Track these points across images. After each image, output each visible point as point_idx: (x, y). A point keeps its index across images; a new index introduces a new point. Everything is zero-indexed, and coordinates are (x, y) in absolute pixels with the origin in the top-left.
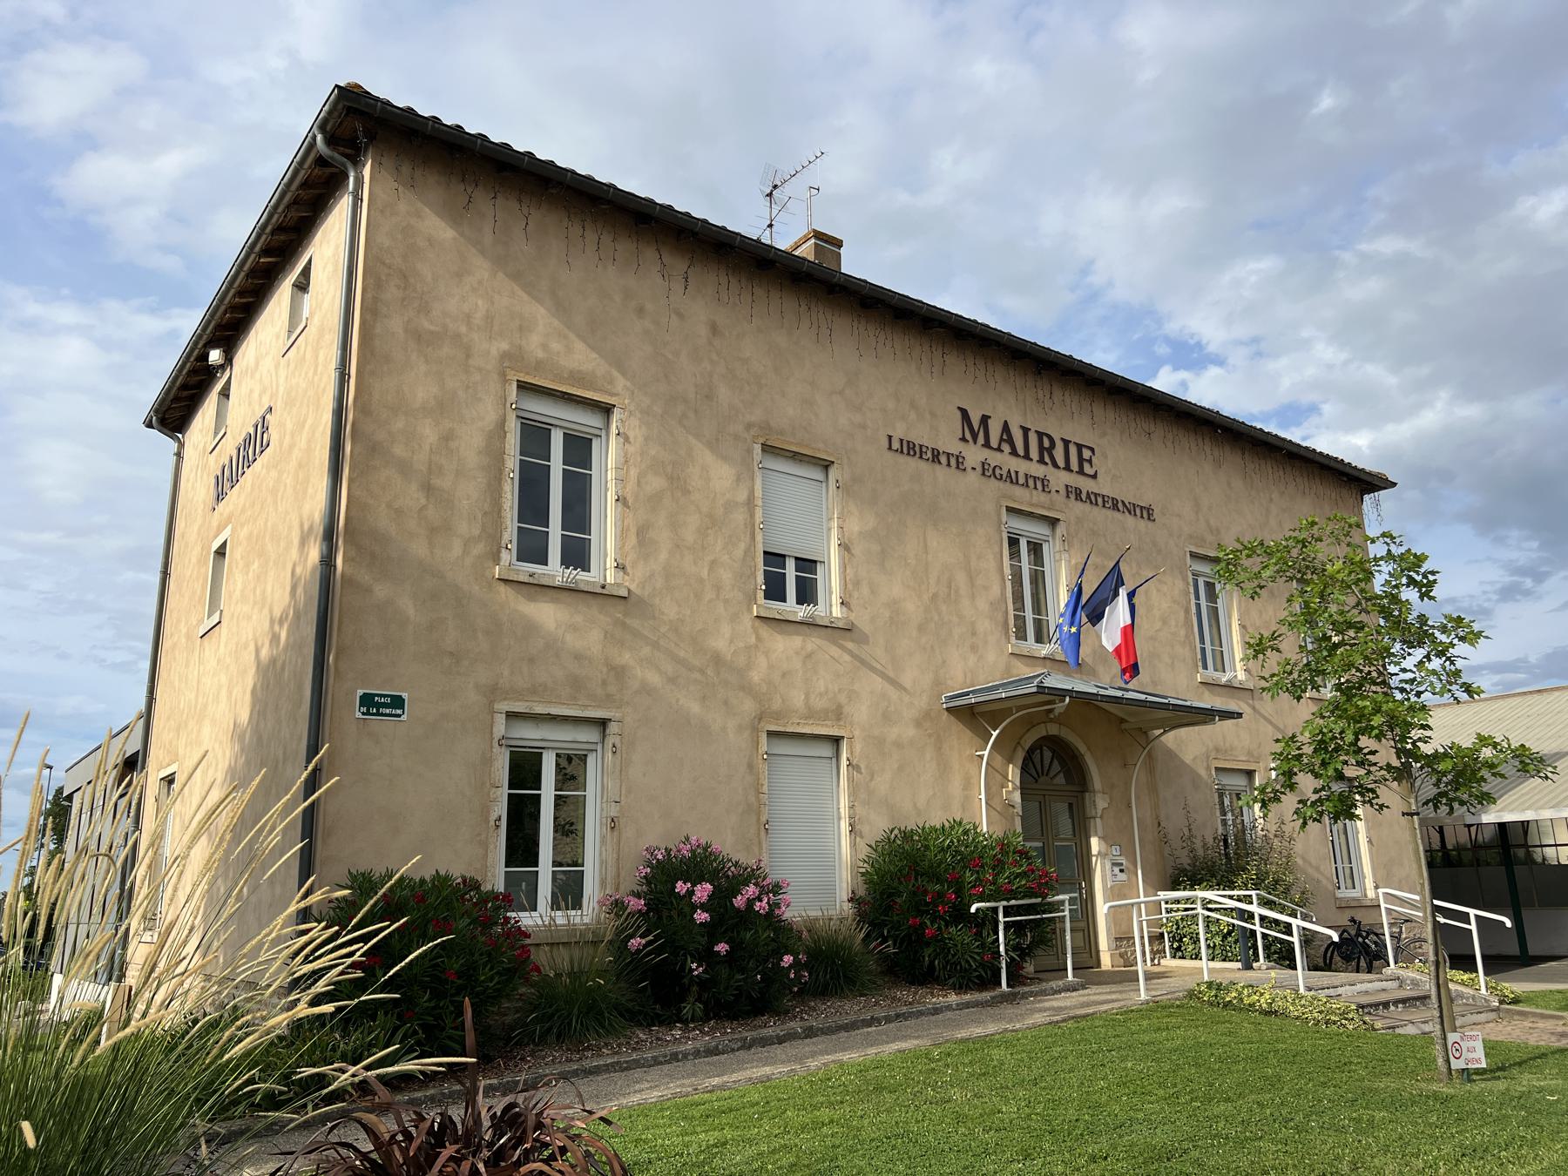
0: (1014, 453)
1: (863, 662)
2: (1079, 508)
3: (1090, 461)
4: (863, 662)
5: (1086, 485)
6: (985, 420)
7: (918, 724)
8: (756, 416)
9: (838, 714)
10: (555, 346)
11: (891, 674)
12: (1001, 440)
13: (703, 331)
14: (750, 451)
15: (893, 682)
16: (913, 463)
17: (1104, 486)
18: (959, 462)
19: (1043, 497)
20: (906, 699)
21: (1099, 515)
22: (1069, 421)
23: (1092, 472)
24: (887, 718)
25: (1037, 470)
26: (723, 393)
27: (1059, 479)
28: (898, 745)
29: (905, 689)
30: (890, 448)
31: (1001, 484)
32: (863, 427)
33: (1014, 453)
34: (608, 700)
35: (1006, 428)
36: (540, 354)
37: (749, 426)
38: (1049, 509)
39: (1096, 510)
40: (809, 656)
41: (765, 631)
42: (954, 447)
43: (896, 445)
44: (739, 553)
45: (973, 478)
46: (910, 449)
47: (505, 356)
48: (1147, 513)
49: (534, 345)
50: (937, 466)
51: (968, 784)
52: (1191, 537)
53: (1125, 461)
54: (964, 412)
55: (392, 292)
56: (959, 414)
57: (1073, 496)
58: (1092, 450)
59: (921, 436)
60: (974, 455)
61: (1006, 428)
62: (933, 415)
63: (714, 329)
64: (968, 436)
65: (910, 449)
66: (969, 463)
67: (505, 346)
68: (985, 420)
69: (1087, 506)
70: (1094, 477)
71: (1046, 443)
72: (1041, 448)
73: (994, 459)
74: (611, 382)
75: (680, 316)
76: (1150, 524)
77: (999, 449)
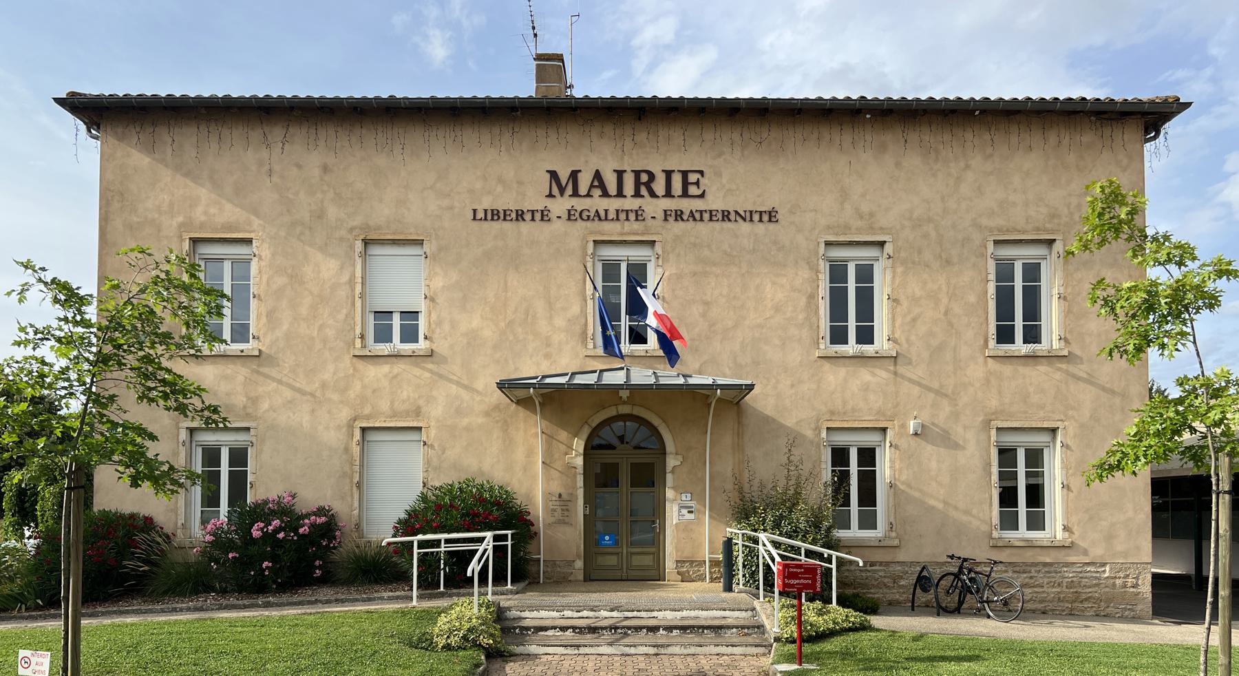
0: (605, 194)
1: (441, 376)
2: (677, 227)
3: (697, 183)
4: (441, 376)
5: (687, 205)
6: (574, 175)
7: (487, 414)
8: (358, 221)
9: (418, 412)
10: (212, 211)
11: (466, 382)
12: (592, 186)
13: (317, 172)
14: (352, 247)
15: (466, 387)
16: (497, 226)
17: (715, 202)
18: (544, 216)
19: (636, 226)
20: (478, 398)
21: (704, 228)
22: (663, 154)
23: (699, 192)
24: (459, 412)
25: (630, 203)
26: (332, 212)
27: (655, 207)
28: (468, 429)
29: (477, 392)
30: (474, 219)
31: (589, 224)
32: (451, 208)
33: (605, 194)
34: (248, 416)
35: (598, 175)
36: (203, 218)
37: (351, 230)
38: (643, 234)
39: (700, 225)
40: (395, 377)
41: (360, 364)
42: (539, 203)
43: (481, 215)
44: (341, 316)
45: (558, 226)
46: (494, 215)
47: (181, 225)
48: (772, 216)
49: (199, 215)
50: (522, 224)
51: (530, 453)
52: (829, 227)
53: (733, 173)
54: (554, 175)
55: (116, 205)
56: (548, 175)
57: (671, 219)
58: (701, 173)
59: (508, 202)
60: (559, 206)
61: (598, 175)
62: (520, 183)
63: (325, 169)
64: (555, 191)
65: (494, 215)
66: (553, 216)
67: (181, 219)
68: (574, 175)
69: (691, 224)
70: (702, 196)
71: (644, 178)
72: (638, 184)
73: (579, 204)
74: (250, 224)
75: (299, 166)
76: (772, 226)
77: (588, 195)
